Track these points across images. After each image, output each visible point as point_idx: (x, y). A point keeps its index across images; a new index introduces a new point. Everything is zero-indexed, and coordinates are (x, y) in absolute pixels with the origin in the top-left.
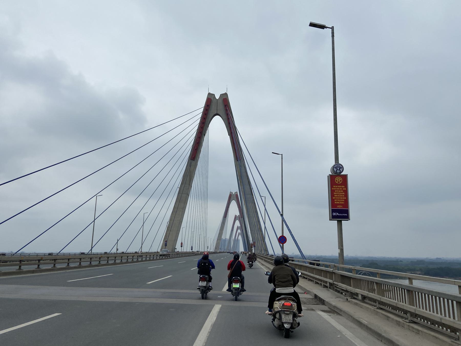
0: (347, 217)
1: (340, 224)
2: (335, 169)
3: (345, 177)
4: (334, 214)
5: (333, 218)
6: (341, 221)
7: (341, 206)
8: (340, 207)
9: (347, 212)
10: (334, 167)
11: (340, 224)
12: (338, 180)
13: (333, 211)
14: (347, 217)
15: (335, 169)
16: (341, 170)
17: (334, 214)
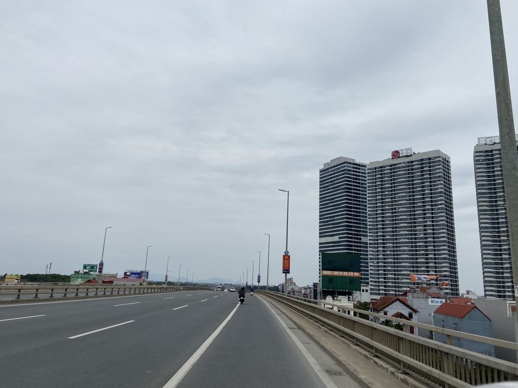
0: (289, 273)
1: (286, 275)
2: (286, 253)
3: (289, 256)
4: (284, 271)
5: (284, 273)
6: (286, 274)
7: (287, 268)
8: (286, 269)
9: (289, 270)
10: (285, 252)
11: (286, 275)
12: (286, 257)
13: (284, 270)
14: (289, 273)
15: (286, 253)
16: (288, 253)
17: (284, 271)
